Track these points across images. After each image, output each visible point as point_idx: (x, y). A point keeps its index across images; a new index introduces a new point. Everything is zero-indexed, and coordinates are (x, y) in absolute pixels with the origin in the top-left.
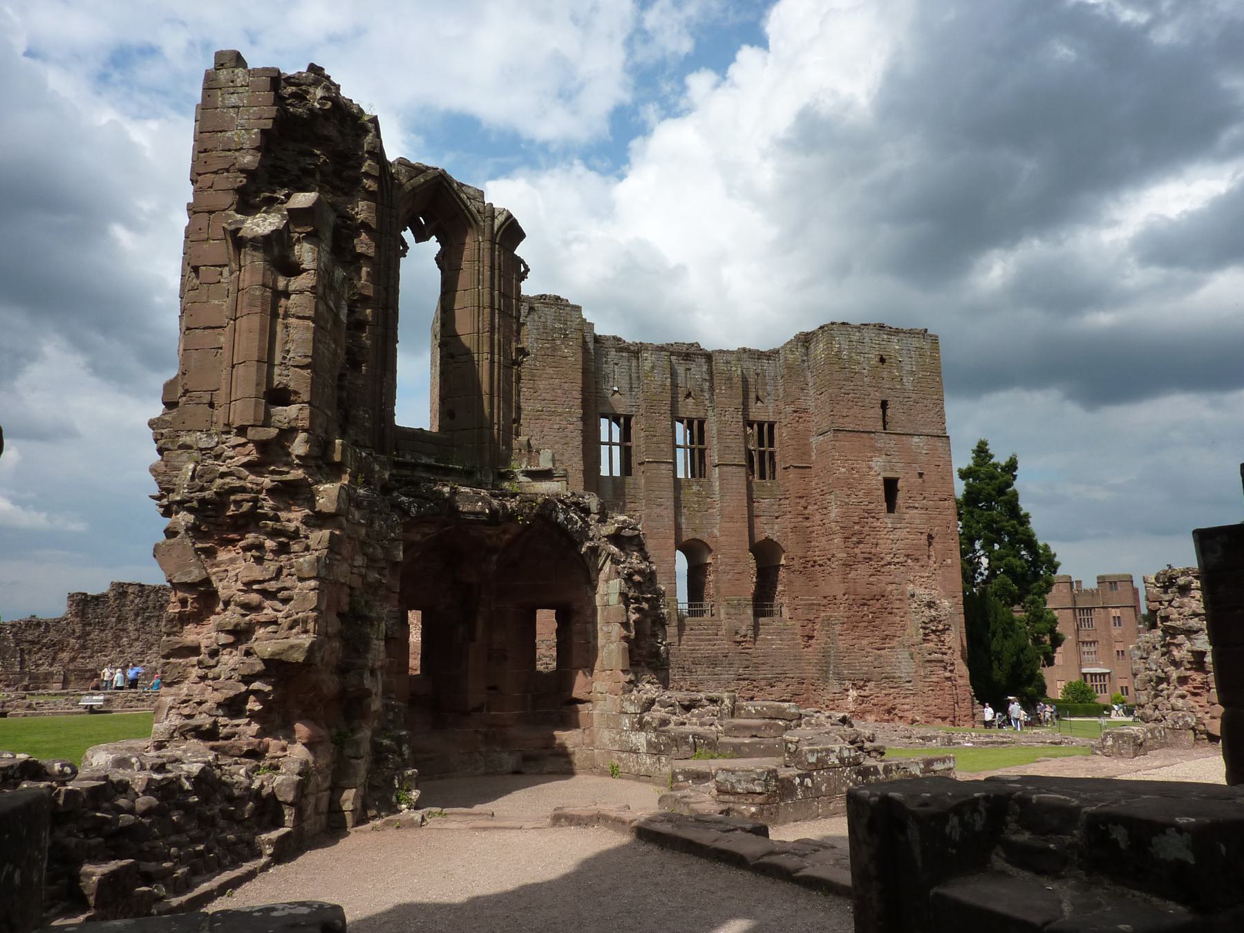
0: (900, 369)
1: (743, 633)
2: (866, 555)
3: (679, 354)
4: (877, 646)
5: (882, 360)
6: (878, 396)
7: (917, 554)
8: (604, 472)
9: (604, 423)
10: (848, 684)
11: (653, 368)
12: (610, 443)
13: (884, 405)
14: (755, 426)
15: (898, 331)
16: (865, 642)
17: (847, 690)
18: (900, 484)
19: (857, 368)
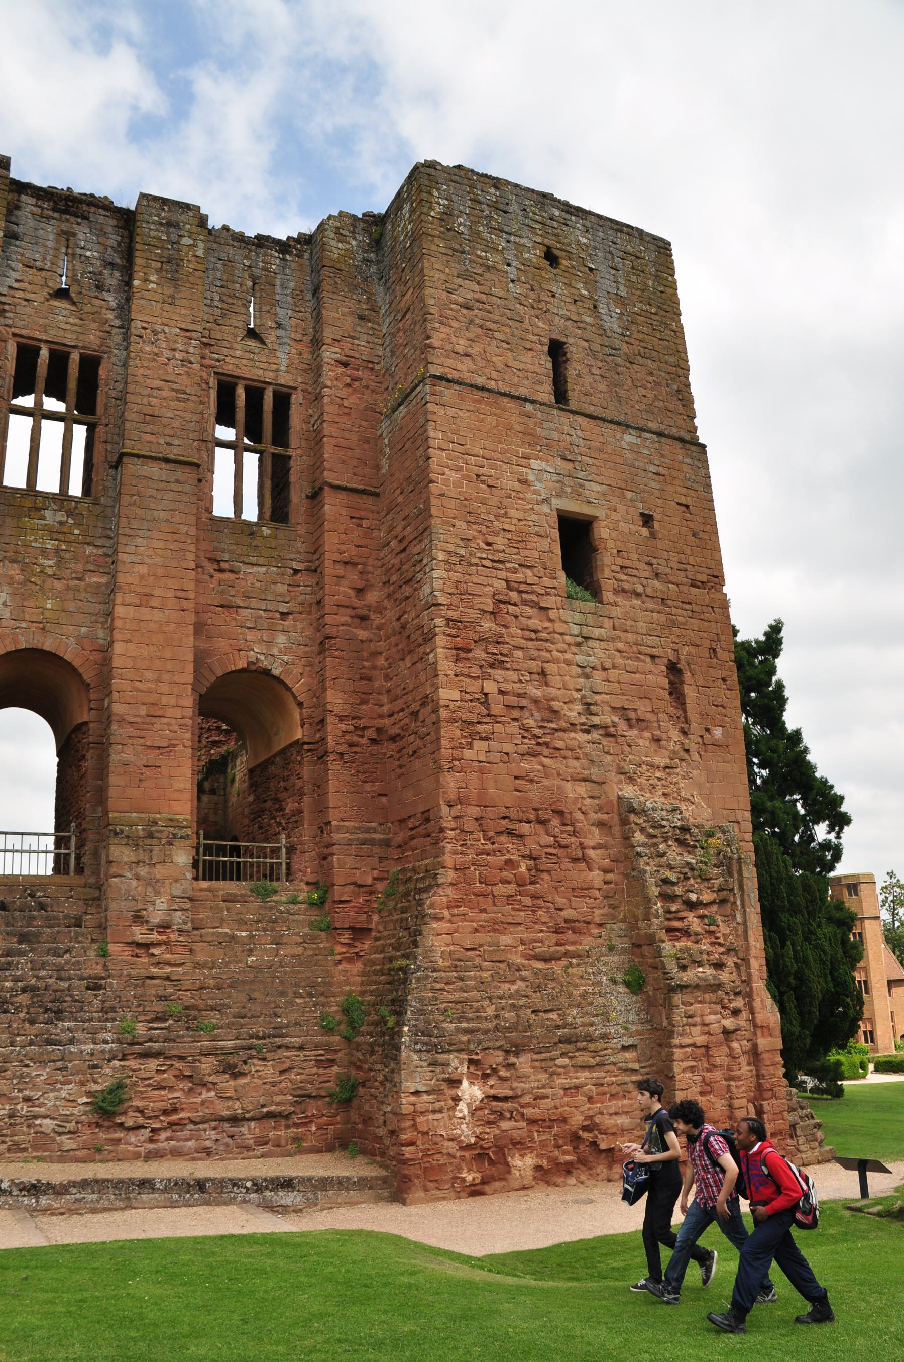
1: (156, 919)
2: (513, 700)
4: (541, 949)
6: (543, 330)
7: (643, 708)
10: (457, 1064)
13: (557, 350)
14: (241, 392)
16: (505, 940)
17: (455, 1083)
18: (602, 532)
19: (493, 258)
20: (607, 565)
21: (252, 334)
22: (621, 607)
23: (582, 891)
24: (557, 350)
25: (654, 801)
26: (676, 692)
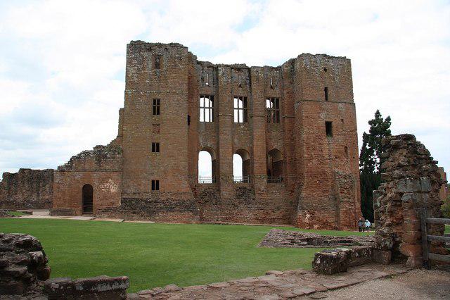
0: (333, 74)
1: (262, 189)
3: (235, 69)
5: (325, 70)
8: (202, 119)
9: (236, 100)
11: (223, 74)
12: (238, 109)
13: (326, 89)
15: (332, 57)
18: (333, 124)
20: (334, 131)
21: (271, 87)
22: (336, 137)
23: (328, 186)
24: (326, 89)
25: (341, 172)
26: (346, 151)
